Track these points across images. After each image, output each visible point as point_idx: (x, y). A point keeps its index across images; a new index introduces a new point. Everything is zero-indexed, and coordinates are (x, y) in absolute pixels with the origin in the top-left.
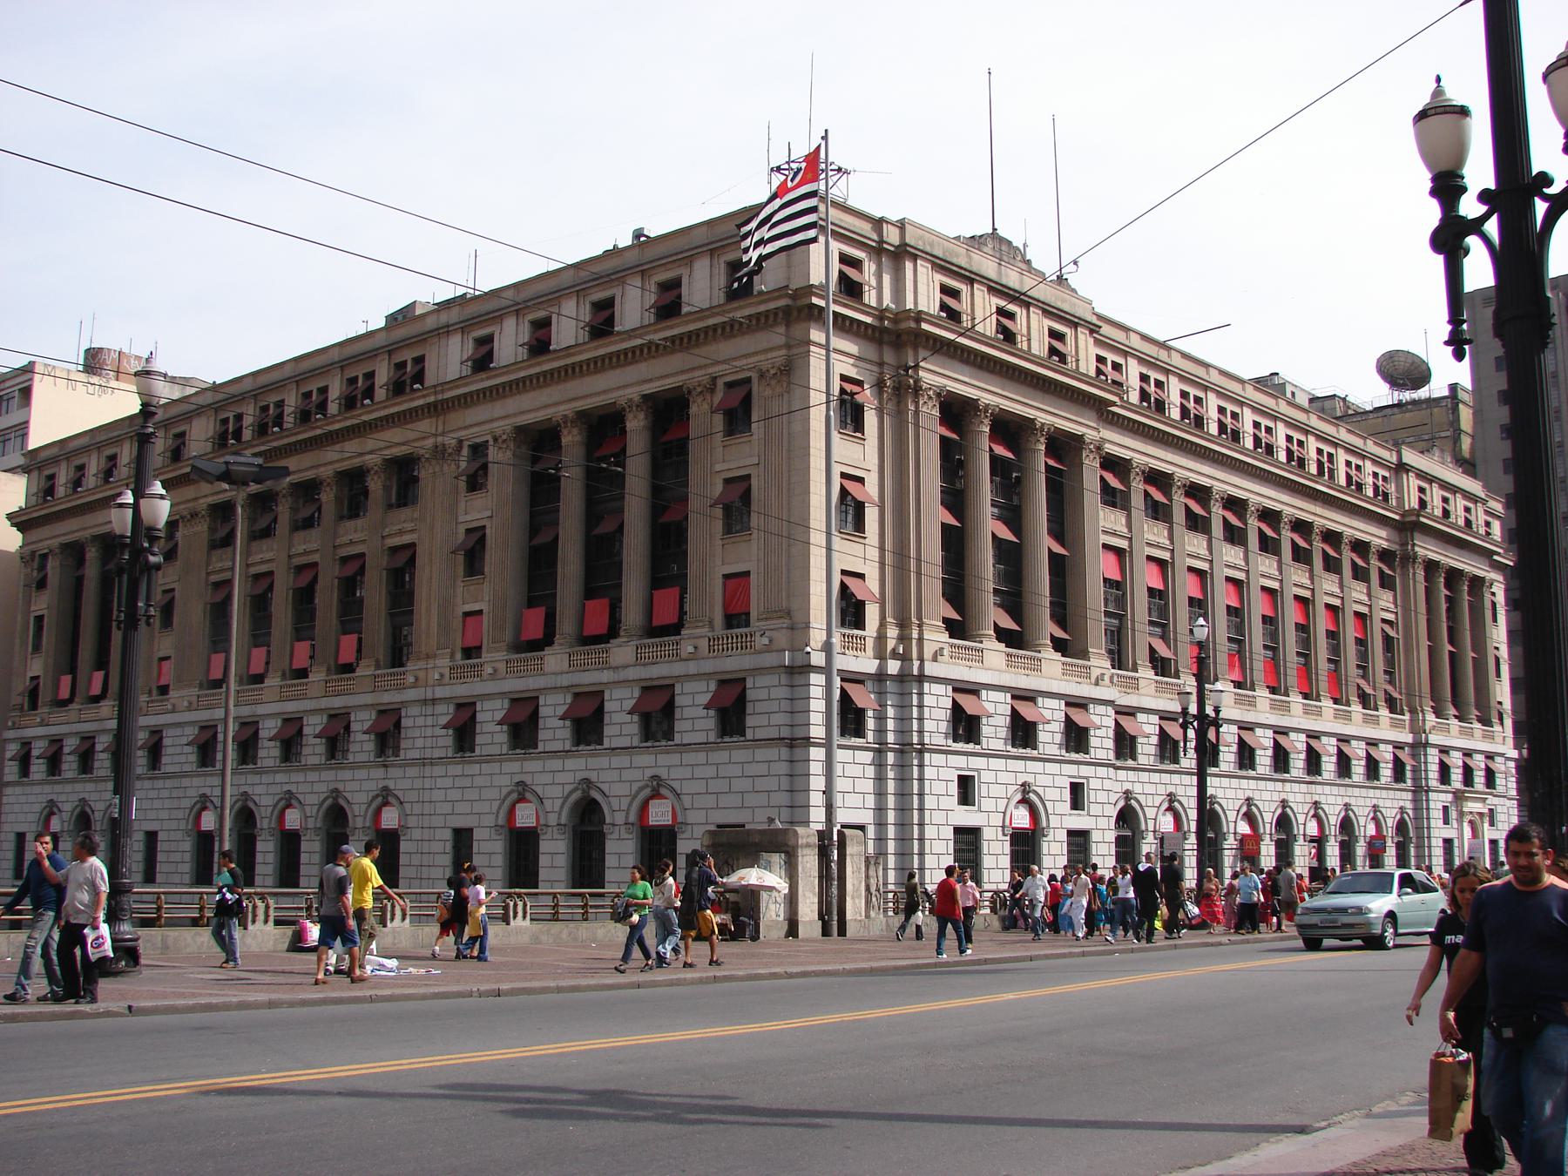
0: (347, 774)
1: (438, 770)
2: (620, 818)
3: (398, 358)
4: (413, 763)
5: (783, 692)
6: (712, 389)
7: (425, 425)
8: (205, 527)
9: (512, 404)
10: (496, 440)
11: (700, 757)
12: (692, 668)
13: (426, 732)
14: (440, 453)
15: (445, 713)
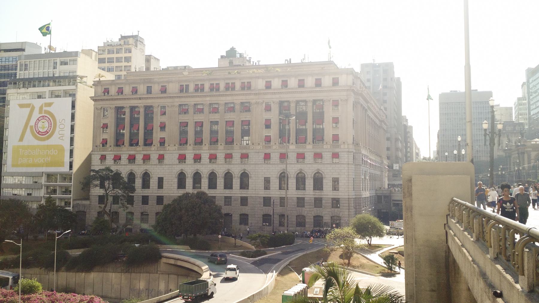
0: (232, 166)
1: (260, 166)
2: (309, 176)
3: (243, 81)
4: (252, 164)
5: (347, 156)
6: (330, 101)
7: (252, 97)
8: (177, 109)
9: (277, 96)
10: (274, 103)
11: (329, 166)
12: (327, 150)
13: (256, 157)
14: (257, 103)
15: (262, 156)
